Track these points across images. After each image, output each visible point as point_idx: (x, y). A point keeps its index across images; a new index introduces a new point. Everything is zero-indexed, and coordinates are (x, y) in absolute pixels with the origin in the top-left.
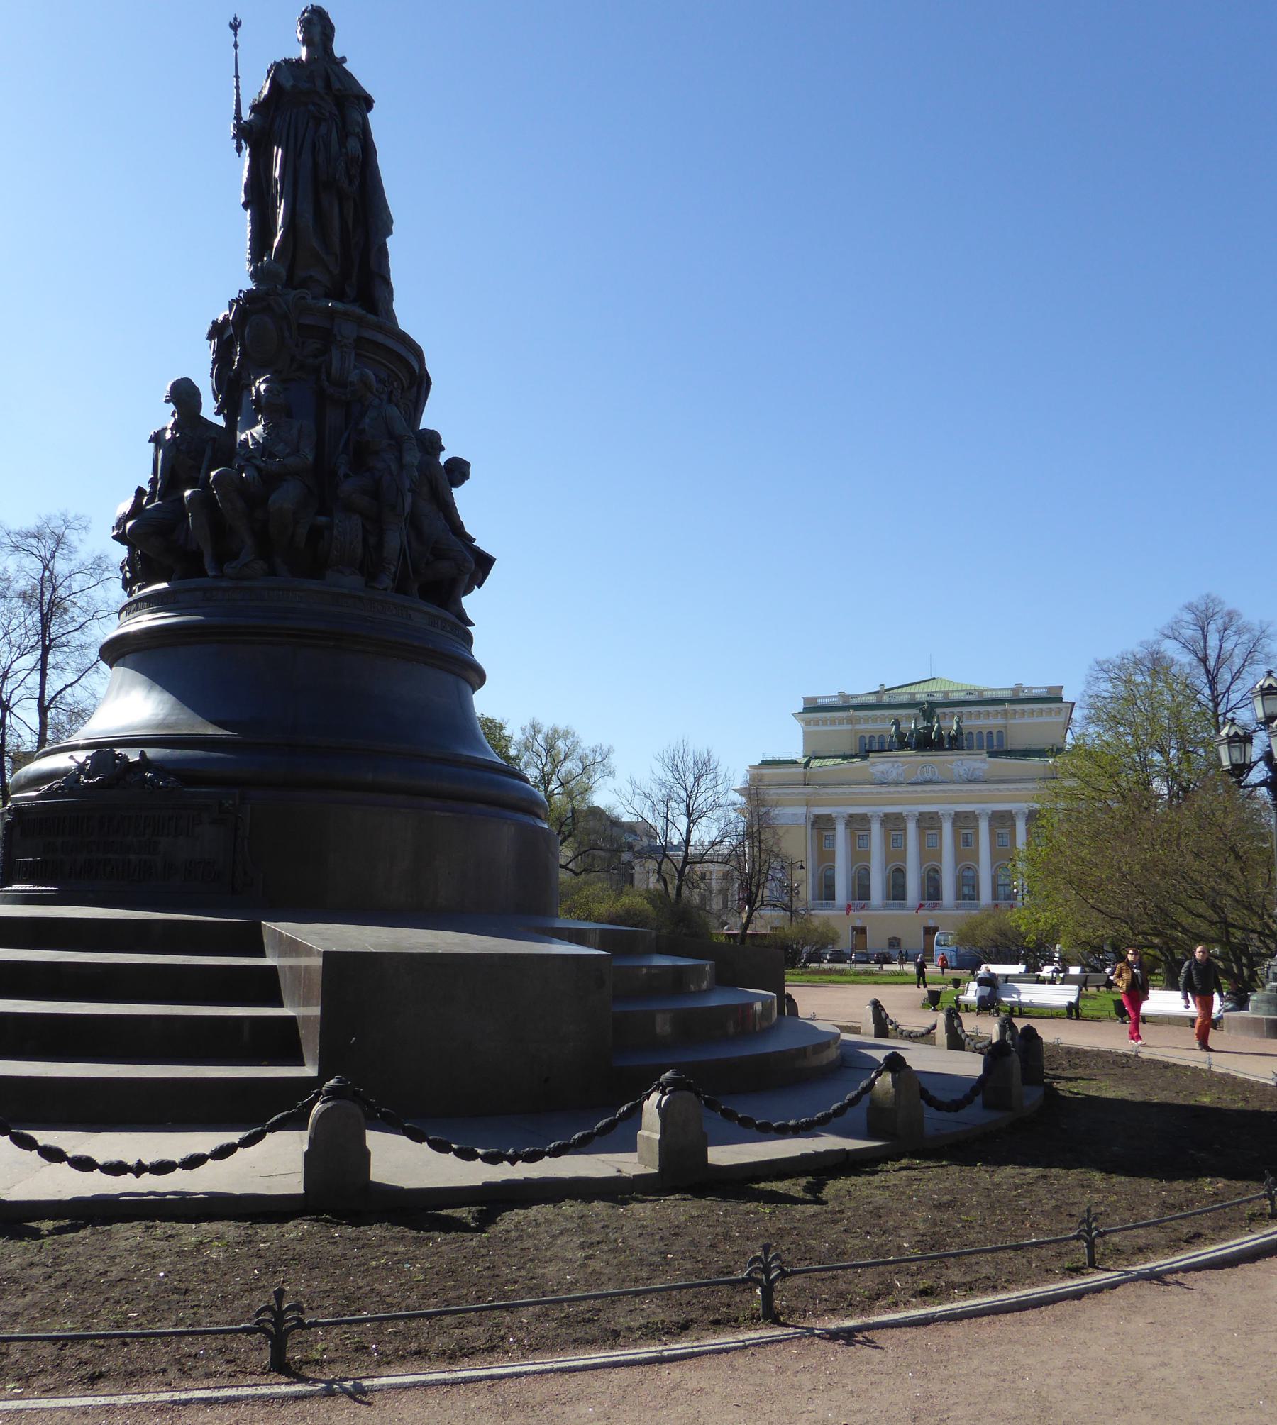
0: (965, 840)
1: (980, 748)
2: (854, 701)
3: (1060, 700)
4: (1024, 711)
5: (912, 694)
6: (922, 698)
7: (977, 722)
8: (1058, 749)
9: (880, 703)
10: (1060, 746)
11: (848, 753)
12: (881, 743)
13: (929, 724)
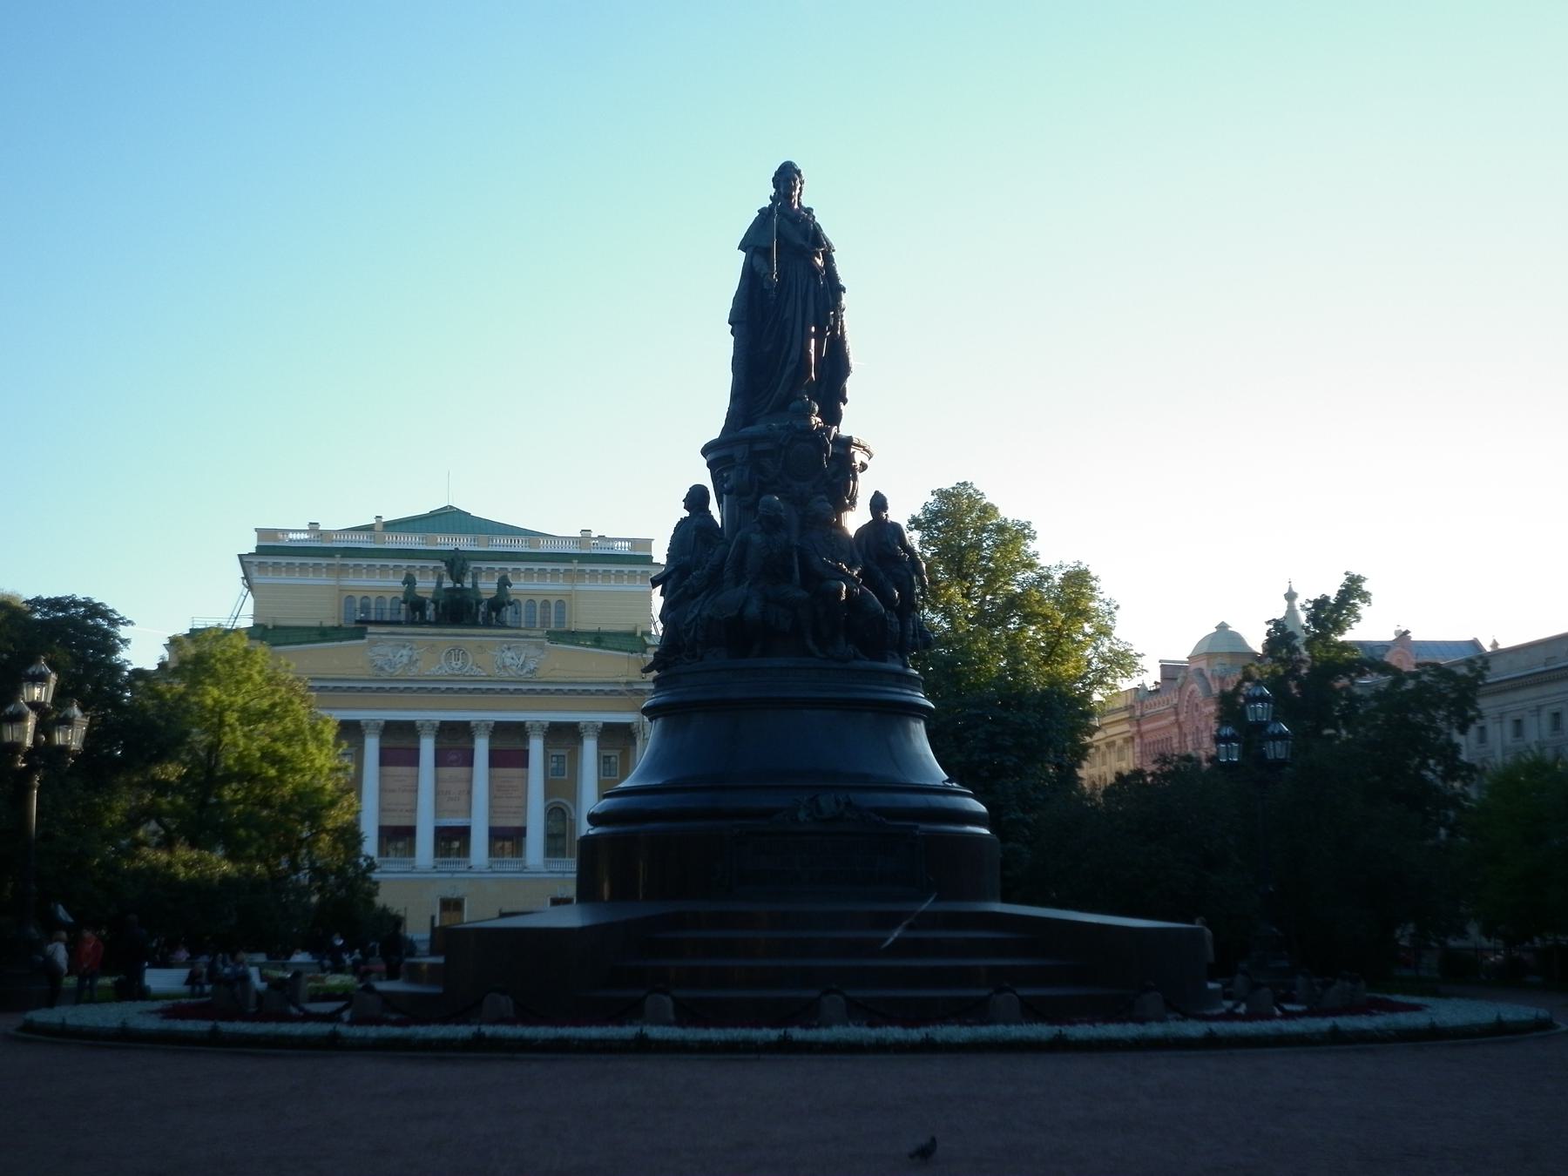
10: (646, 629)
11: (328, 623)
13: (458, 585)
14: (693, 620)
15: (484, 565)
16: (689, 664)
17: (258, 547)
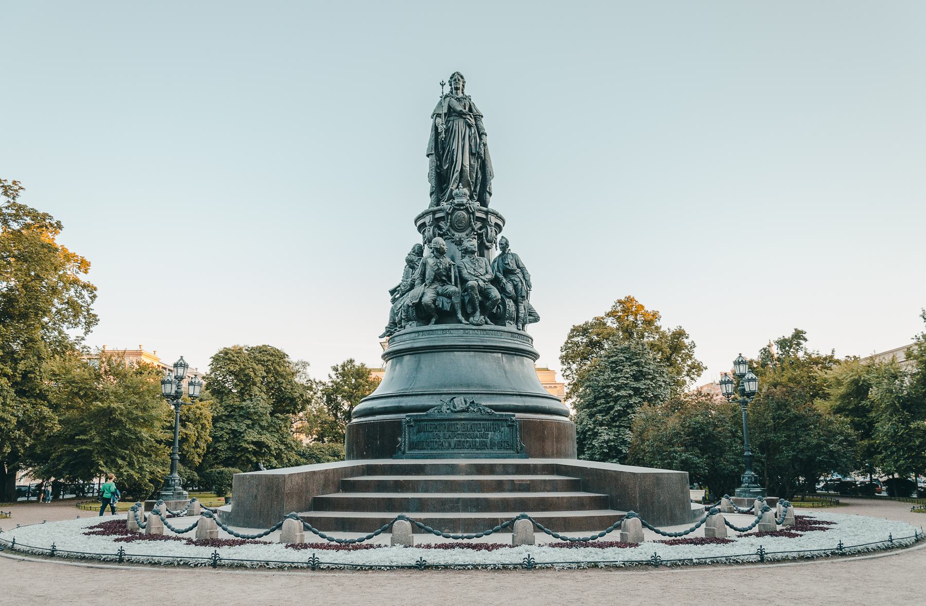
14: (401, 307)
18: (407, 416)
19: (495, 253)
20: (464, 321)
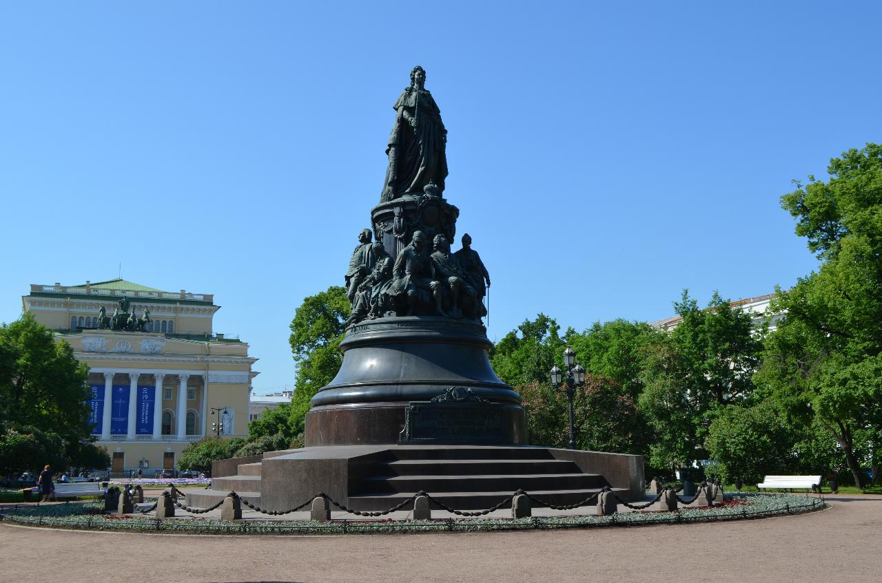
0: (170, 394)
1: (157, 331)
2: (69, 291)
3: (211, 304)
4: (188, 309)
5: (113, 291)
6: (118, 293)
7: (158, 314)
8: (208, 336)
9: (87, 294)
10: (210, 334)
11: (63, 328)
12: (88, 323)
15: (137, 304)
16: (372, 319)
17: (31, 293)
18: (412, 404)
19: (456, 247)
20: (445, 315)
